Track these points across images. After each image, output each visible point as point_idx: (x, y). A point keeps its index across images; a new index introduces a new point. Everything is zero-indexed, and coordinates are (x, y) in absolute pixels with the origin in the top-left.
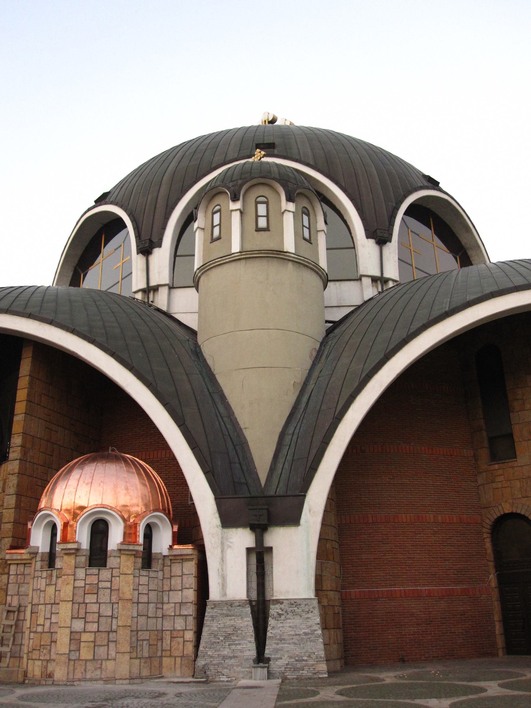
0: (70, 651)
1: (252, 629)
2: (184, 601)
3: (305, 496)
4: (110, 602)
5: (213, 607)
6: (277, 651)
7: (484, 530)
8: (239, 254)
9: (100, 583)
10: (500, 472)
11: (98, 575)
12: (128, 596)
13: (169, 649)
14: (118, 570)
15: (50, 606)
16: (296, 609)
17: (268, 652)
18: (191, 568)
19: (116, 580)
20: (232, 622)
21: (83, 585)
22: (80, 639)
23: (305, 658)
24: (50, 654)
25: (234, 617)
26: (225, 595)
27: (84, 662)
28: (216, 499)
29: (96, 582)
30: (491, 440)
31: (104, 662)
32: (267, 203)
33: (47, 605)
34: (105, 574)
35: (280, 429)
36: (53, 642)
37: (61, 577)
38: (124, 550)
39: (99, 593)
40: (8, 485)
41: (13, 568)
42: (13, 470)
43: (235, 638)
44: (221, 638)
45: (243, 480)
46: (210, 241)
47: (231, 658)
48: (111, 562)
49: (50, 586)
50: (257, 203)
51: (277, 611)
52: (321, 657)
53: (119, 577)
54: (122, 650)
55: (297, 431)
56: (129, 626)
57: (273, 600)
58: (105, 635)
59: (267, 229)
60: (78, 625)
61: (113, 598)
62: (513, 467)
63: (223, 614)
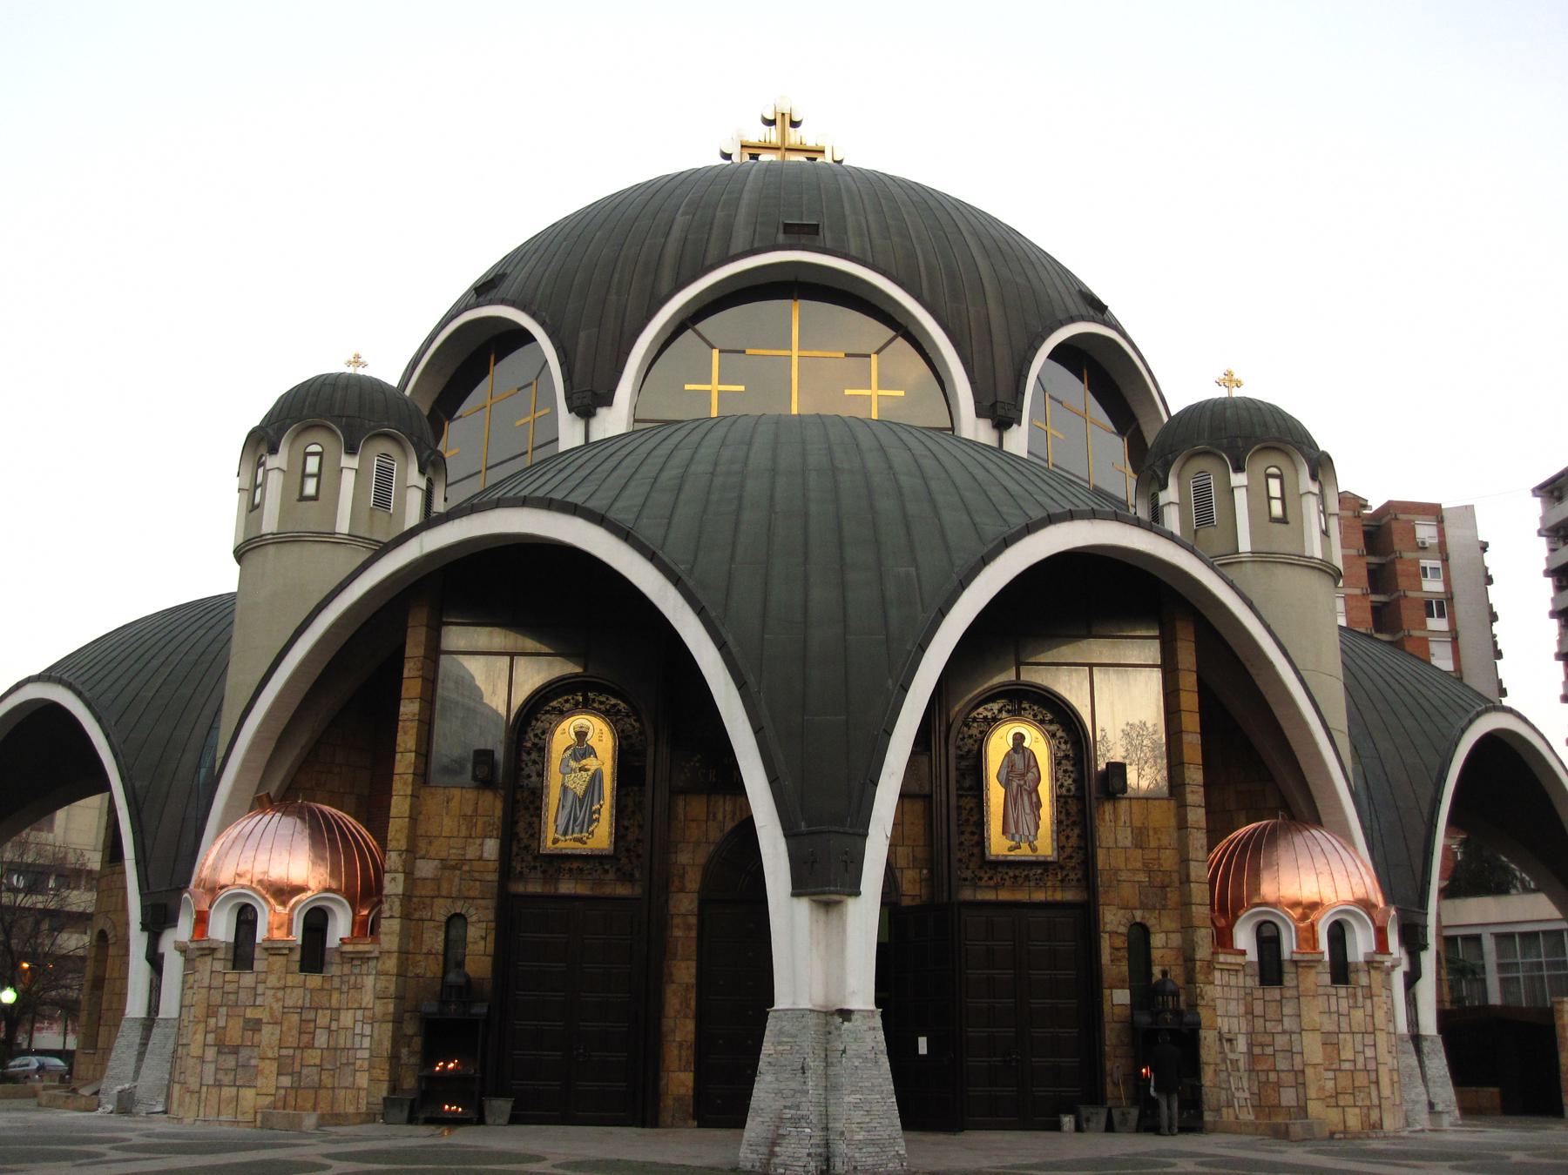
1: (1419, 1070)
8: (1319, 562)
15: (1361, 1035)
24: (1371, 1099)
41: (1217, 974)
46: (1268, 518)
49: (1357, 1009)
55: (1376, 826)
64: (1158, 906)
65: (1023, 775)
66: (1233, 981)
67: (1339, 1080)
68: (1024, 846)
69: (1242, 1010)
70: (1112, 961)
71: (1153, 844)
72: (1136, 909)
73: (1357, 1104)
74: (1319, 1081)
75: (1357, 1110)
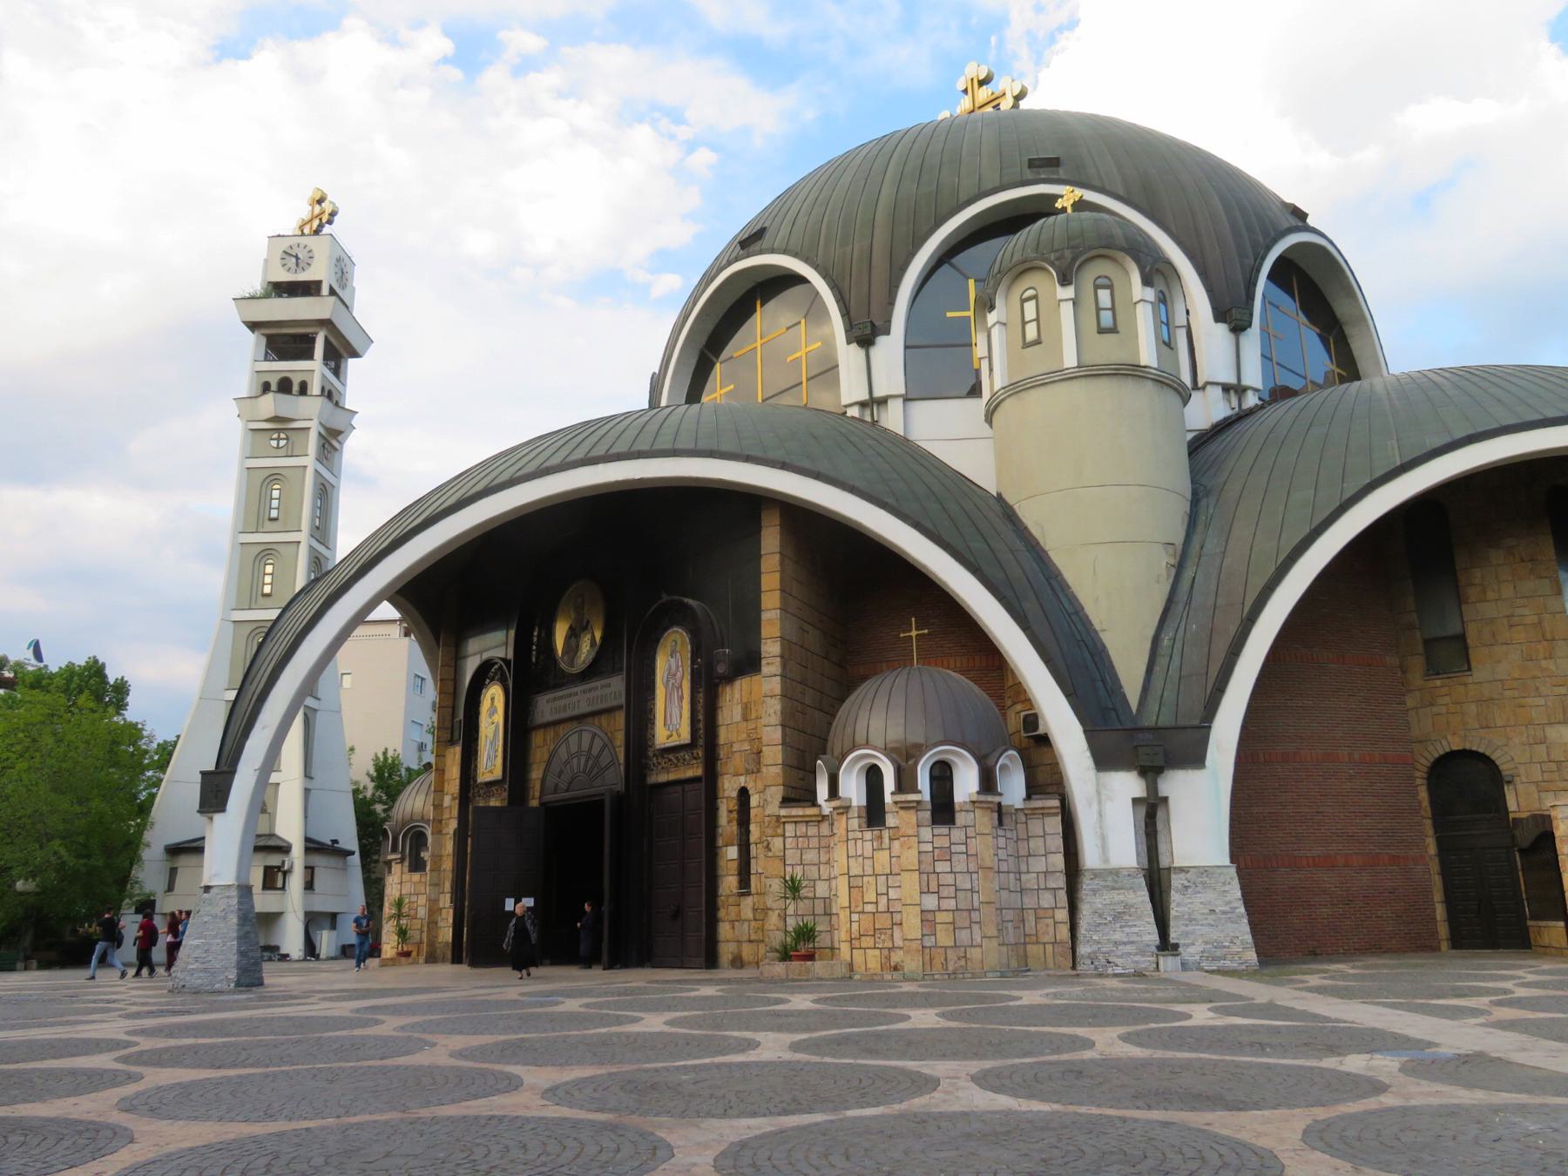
0: (923, 935)
1: (1150, 906)
2: (1049, 870)
3: (1210, 727)
4: (968, 872)
5: (1093, 877)
6: (1186, 934)
7: (1418, 774)
8: (1077, 370)
9: (952, 846)
10: (1445, 690)
11: (949, 835)
12: (988, 863)
13: (1034, 933)
14: (973, 829)
16: (1206, 879)
17: (1173, 937)
18: (1055, 825)
19: (972, 842)
20: (1122, 897)
21: (931, 850)
22: (935, 920)
23: (1228, 944)
25: (1122, 891)
26: (1106, 860)
27: (943, 949)
28: (1085, 731)
29: (948, 845)
30: (1427, 642)
31: (968, 949)
32: (1110, 287)
33: (878, 877)
34: (957, 835)
35: (1151, 632)
36: (896, 924)
37: (898, 839)
38: (981, 802)
39: (953, 860)
40: (766, 712)
42: (772, 690)
43: (1128, 918)
44: (1109, 919)
45: (1111, 706)
46: (1021, 344)
47: (1125, 944)
48: (961, 818)
49: (881, 852)
50: (1097, 287)
51: (1182, 882)
52: (1247, 943)
53: (975, 837)
54: (989, 934)
56: (994, 903)
57: (1175, 868)
58: (965, 914)
59: (1113, 330)
60: (930, 902)
61: (970, 865)
62: (1465, 684)
63: (1108, 886)
64: (755, 770)
65: (675, 675)
66: (812, 831)
67: (862, 922)
68: (674, 733)
69: (824, 858)
70: (729, 822)
71: (753, 716)
72: (742, 775)
73: (877, 946)
74: (847, 923)
75: (877, 952)
